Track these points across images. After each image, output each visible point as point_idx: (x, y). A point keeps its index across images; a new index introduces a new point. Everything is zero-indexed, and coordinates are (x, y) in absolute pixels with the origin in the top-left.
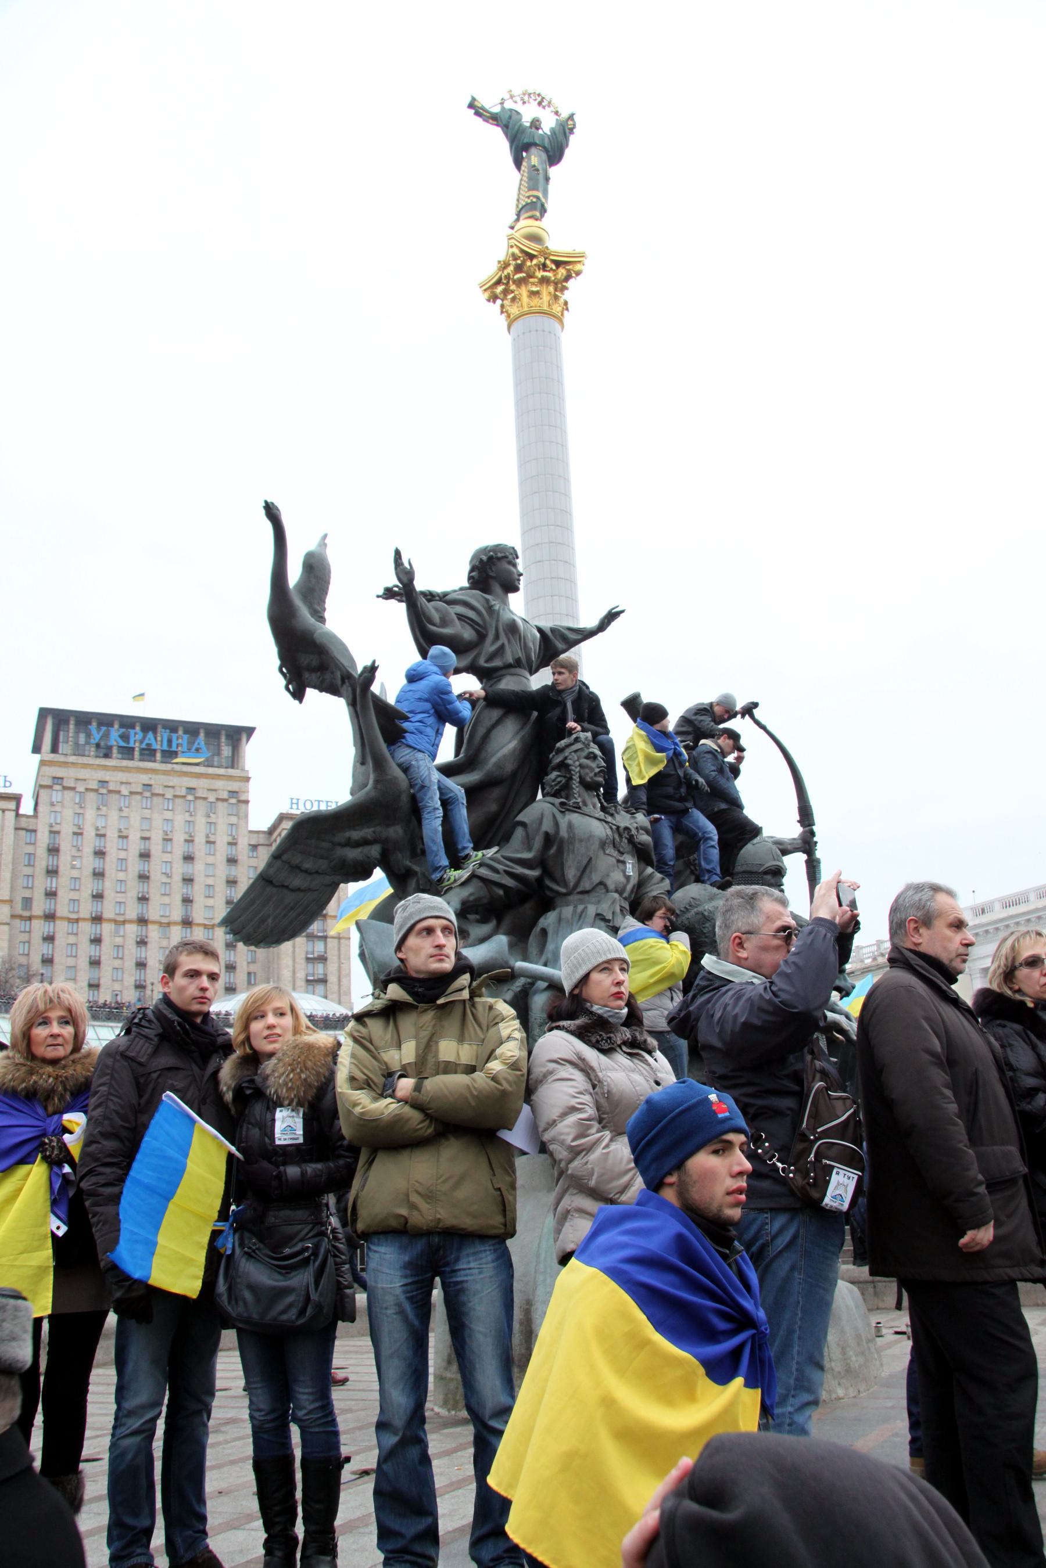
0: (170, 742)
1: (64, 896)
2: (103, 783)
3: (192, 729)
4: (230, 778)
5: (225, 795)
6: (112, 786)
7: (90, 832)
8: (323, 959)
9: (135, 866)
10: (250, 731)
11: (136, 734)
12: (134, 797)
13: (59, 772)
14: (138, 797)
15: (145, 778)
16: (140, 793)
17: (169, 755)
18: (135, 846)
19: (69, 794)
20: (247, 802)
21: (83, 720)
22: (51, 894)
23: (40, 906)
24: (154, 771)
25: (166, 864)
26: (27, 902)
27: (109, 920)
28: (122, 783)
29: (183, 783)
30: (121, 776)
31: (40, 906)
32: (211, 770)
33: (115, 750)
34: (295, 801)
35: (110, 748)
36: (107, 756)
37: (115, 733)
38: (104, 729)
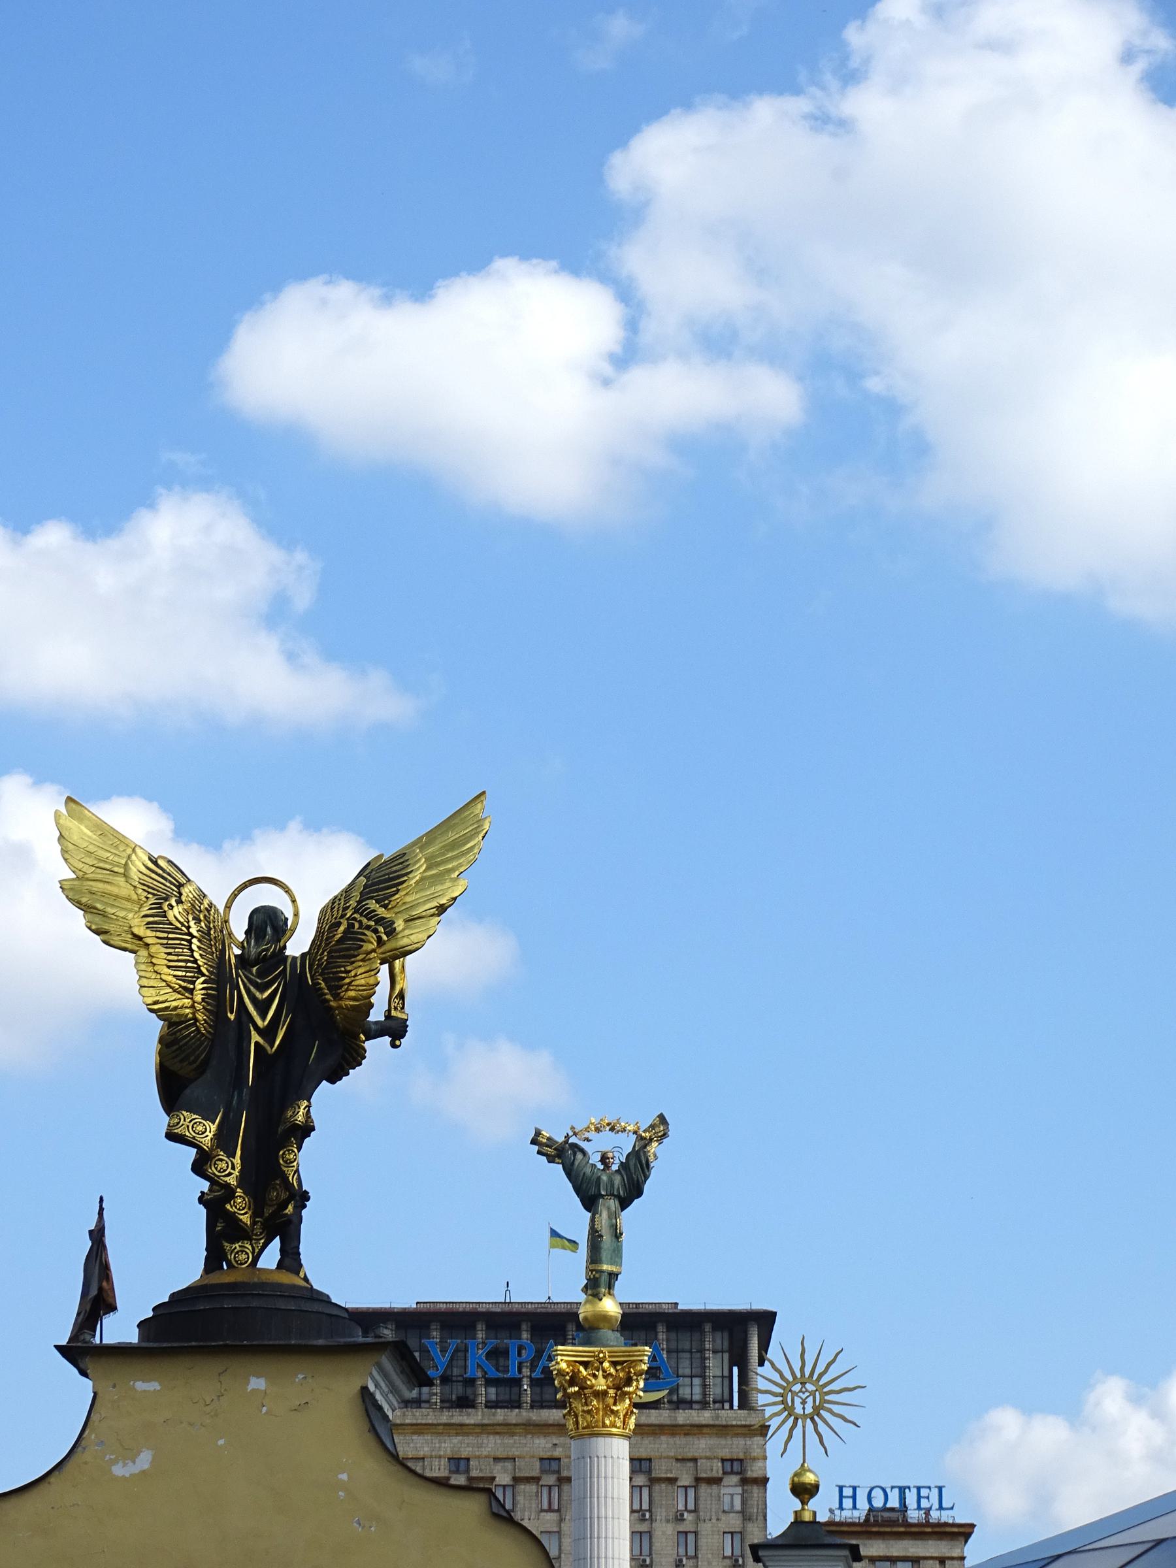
4: (723, 1430)
10: (766, 1320)
11: (520, 1349)
12: (521, 1487)
14: (532, 1488)
15: (542, 1445)
16: (536, 1480)
20: (764, 1481)
28: (497, 1459)
30: (492, 1445)
32: (683, 1417)
34: (848, 1492)
36: (465, 1403)
38: (453, 1343)
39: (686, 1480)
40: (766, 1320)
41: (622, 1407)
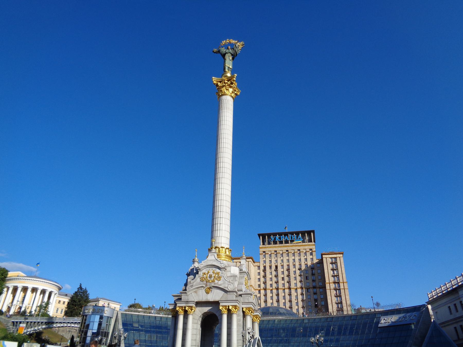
0: (292, 237)
2: (276, 251)
3: (297, 233)
9: (286, 273)
10: (313, 232)
15: (286, 248)
17: (292, 241)
18: (286, 267)
21: (269, 235)
24: (288, 246)
26: (259, 286)
27: (281, 289)
29: (296, 248)
30: (280, 249)
32: (304, 244)
33: (278, 242)
35: (277, 242)
37: (278, 237)
40: (313, 232)
41: (231, 90)
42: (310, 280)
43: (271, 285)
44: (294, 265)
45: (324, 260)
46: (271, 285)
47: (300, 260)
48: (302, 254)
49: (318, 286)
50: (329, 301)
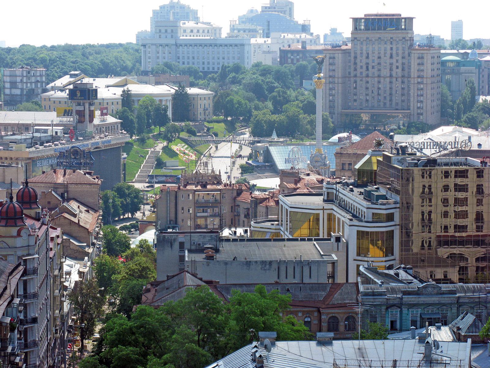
1: (359, 70)
2: (367, 38)
5: (401, 38)
6: (370, 39)
7: (365, 52)
8: (422, 89)
13: (356, 36)
18: (376, 56)
19: (359, 42)
22: (355, 70)
23: (352, 75)
25: (386, 60)
26: (349, 73)
31: (352, 75)
32: (397, 31)
39: (398, 40)
42: (400, 70)
43: (361, 73)
44: (385, 53)
45: (412, 55)
46: (361, 73)
47: (391, 49)
48: (394, 43)
49: (406, 75)
50: (412, 94)
